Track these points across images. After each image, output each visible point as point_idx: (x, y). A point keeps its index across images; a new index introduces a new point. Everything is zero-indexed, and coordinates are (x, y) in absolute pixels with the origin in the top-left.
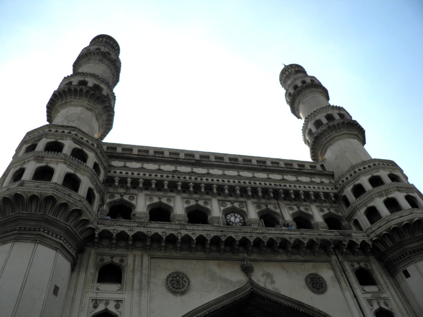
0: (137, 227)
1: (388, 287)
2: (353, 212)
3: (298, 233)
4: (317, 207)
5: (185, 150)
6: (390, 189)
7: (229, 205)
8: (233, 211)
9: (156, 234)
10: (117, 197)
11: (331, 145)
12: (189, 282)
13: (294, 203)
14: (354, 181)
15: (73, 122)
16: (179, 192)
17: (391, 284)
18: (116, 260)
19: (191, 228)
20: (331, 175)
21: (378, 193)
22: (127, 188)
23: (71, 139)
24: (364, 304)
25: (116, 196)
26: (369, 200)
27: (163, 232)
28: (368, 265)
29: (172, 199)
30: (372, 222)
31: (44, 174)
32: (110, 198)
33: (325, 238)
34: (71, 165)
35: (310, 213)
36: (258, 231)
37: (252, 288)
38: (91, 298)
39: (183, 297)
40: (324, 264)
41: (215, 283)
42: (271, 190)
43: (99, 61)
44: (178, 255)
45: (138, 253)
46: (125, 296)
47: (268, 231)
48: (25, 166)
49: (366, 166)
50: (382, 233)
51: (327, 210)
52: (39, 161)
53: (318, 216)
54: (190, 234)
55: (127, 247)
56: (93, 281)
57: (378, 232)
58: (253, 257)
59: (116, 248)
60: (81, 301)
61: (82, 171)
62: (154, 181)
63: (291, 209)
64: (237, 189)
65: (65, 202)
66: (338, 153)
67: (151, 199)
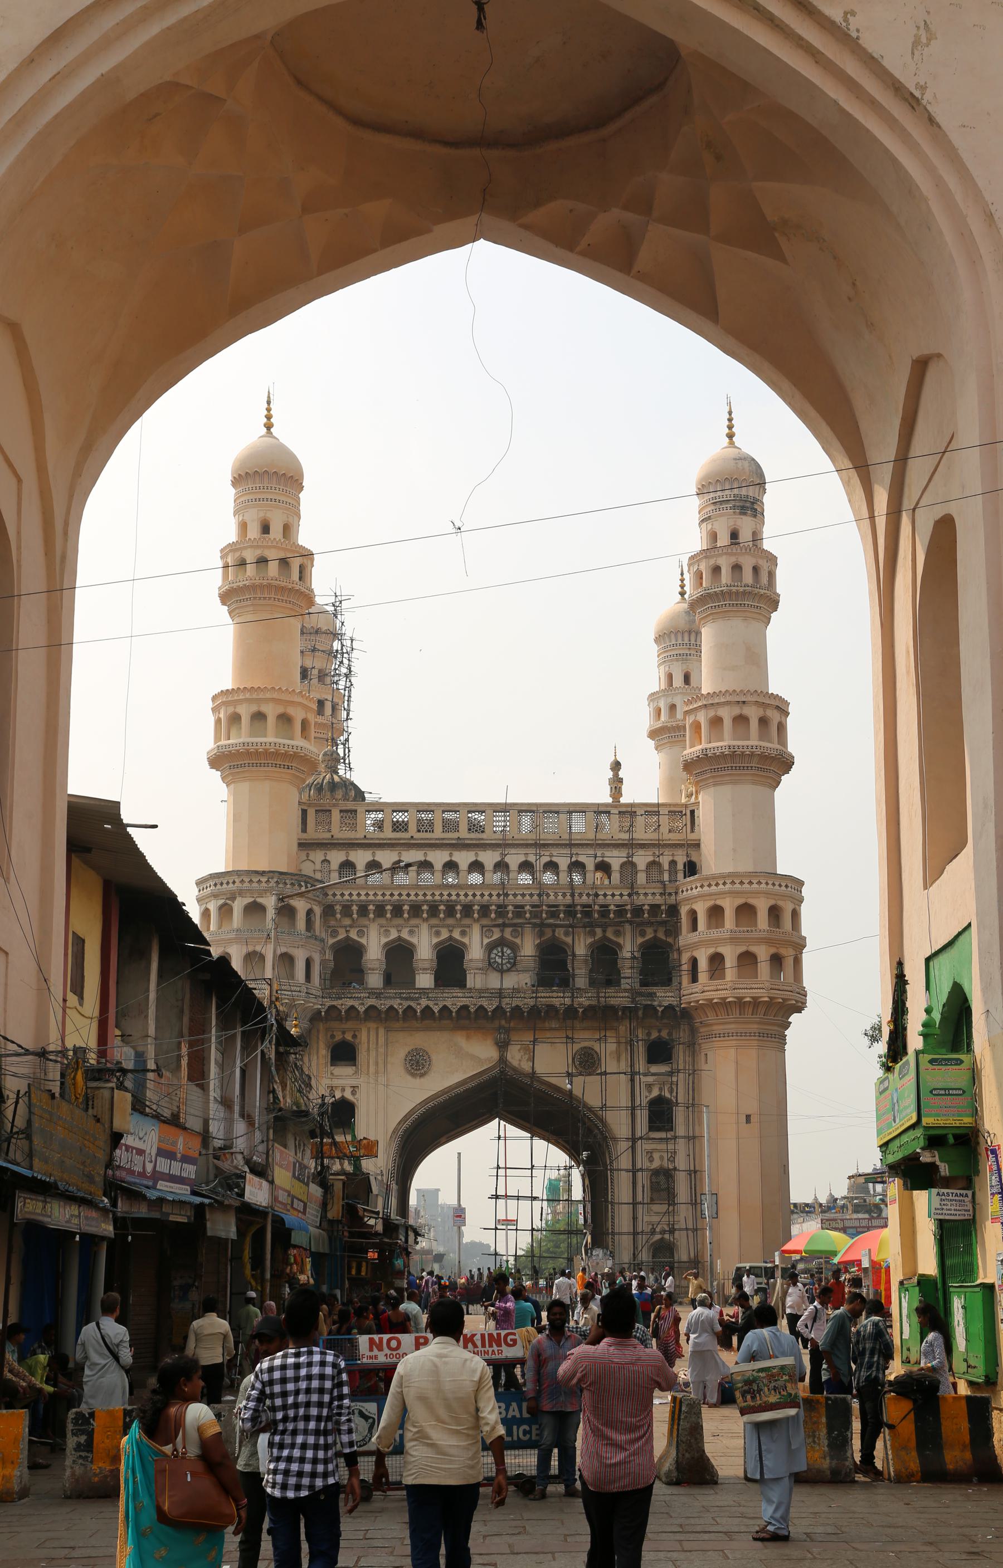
7: (496, 935)
9: (391, 1008)
12: (430, 1061)
18: (349, 1037)
20: (697, 845)
27: (400, 1004)
35: (621, 941)
39: (422, 1079)
41: (460, 1061)
42: (561, 908)
45: (372, 1025)
46: (361, 1081)
53: (629, 946)
54: (431, 1004)
56: (326, 1066)
58: (512, 1025)
63: (593, 934)
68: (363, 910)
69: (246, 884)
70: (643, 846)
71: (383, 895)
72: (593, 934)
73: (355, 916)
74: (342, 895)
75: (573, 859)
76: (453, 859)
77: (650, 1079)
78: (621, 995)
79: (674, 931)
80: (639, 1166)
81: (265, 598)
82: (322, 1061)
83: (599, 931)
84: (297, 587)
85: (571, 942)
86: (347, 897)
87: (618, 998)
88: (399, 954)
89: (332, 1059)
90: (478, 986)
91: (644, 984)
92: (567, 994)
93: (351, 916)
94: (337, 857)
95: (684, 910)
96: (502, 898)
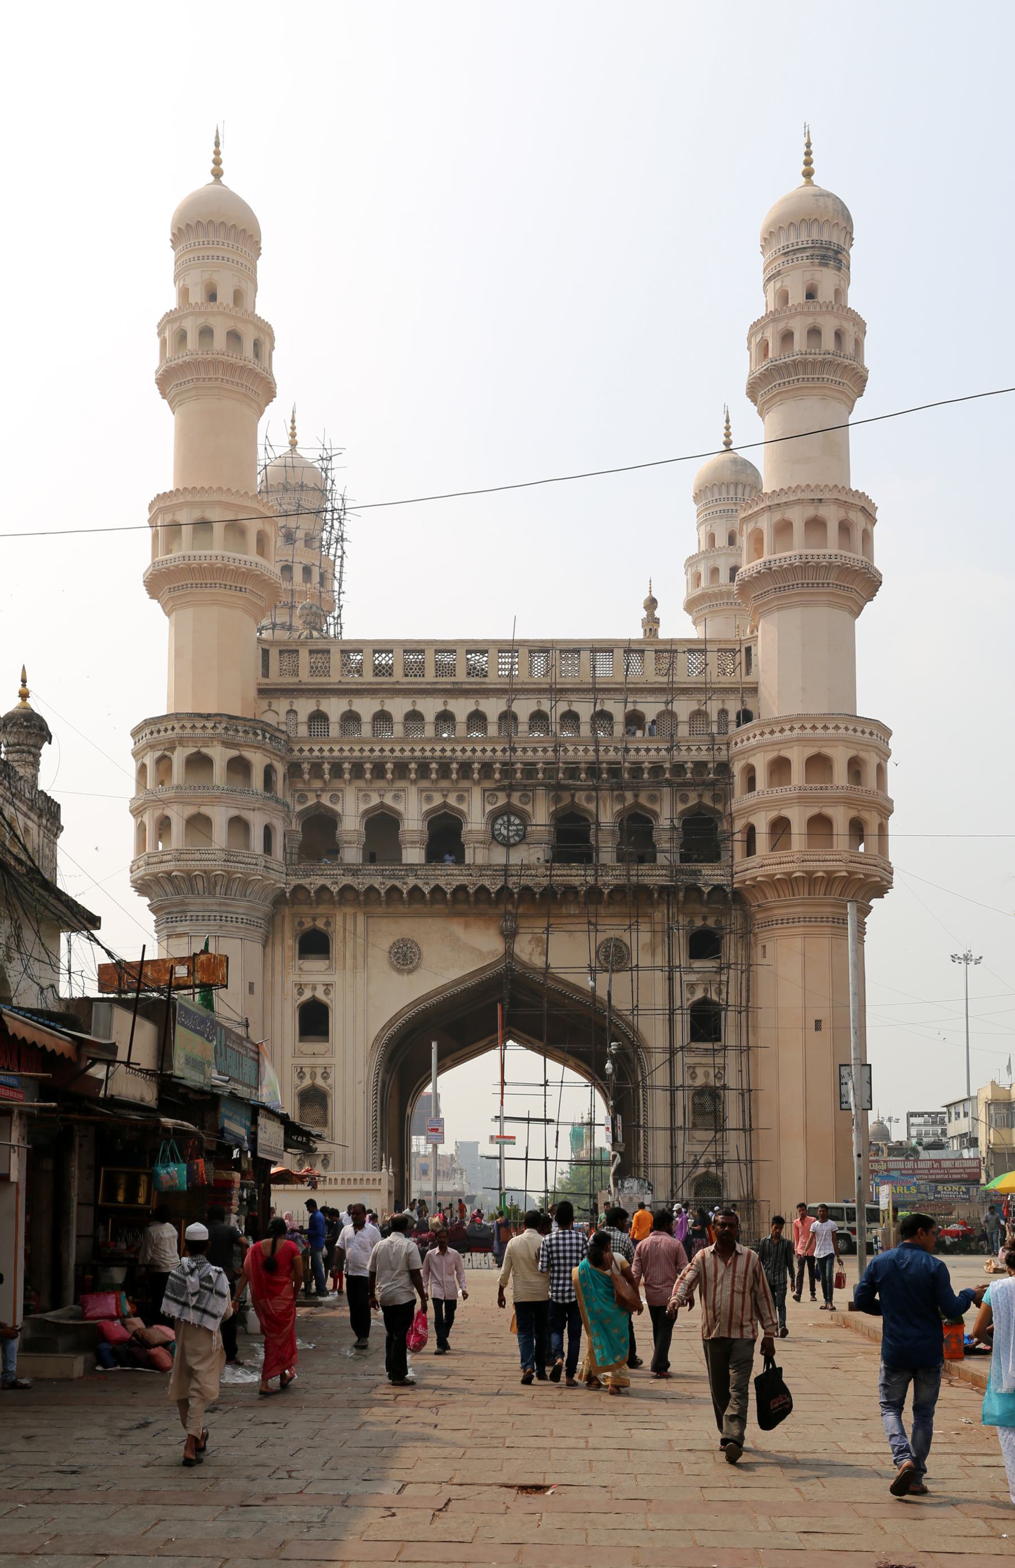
5: (436, 641)
7: (502, 800)
10: (312, 801)
12: (420, 954)
16: (414, 782)
18: (320, 924)
20: (754, 690)
29: (402, 794)
35: (656, 808)
36: (529, 872)
39: (411, 976)
41: (456, 955)
45: (349, 910)
46: (335, 978)
53: (666, 813)
54: (420, 883)
55: (331, 901)
58: (520, 910)
63: (621, 799)
68: (337, 770)
69: (188, 731)
70: (685, 691)
71: (362, 750)
72: (621, 799)
73: (327, 776)
74: (311, 750)
75: (598, 708)
76: (449, 708)
77: (693, 978)
78: (657, 872)
79: (724, 795)
80: (679, 1082)
81: (210, 379)
83: (629, 795)
84: (251, 366)
85: (594, 810)
86: (316, 753)
87: (653, 876)
88: (382, 826)
90: (480, 860)
91: (685, 858)
92: (589, 872)
93: (322, 777)
94: (305, 707)
95: (737, 768)
96: (508, 754)
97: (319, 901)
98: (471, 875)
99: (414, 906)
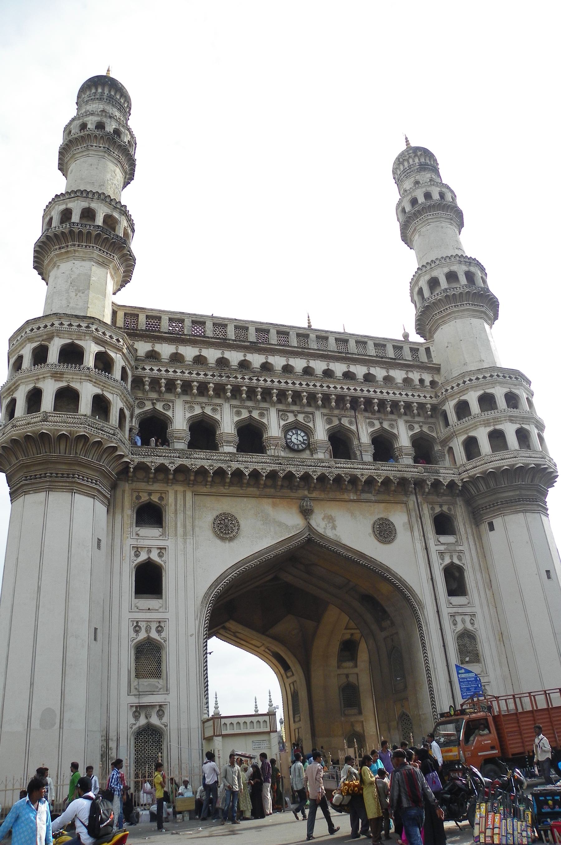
0: (179, 457)
1: (467, 538)
2: (449, 438)
3: (373, 467)
4: (406, 422)
5: (236, 320)
6: (500, 417)
7: (291, 418)
8: (295, 426)
9: (202, 467)
10: (148, 406)
11: (444, 323)
13: (377, 415)
14: (461, 394)
15: (83, 293)
16: (227, 399)
17: (473, 535)
19: (244, 459)
20: (437, 369)
21: (484, 421)
22: (160, 392)
23: (91, 338)
24: (434, 557)
25: (146, 405)
26: (472, 428)
28: (452, 508)
30: (469, 456)
31: (67, 398)
32: (139, 407)
33: (405, 476)
34: (98, 382)
35: (395, 431)
36: (324, 464)
37: (309, 534)
38: (132, 546)
39: (232, 544)
40: (399, 506)
42: (348, 398)
43: (105, 152)
44: (225, 491)
45: (180, 488)
46: (168, 543)
47: (336, 463)
48: (40, 385)
49: (480, 376)
50: (476, 474)
51: (418, 427)
52: (58, 379)
54: (241, 467)
55: (166, 481)
57: (472, 473)
58: (314, 495)
59: (154, 482)
60: (121, 548)
61: (111, 388)
62: (195, 383)
63: (372, 424)
64: (304, 396)
65: (100, 440)
66: (453, 331)
67: (191, 408)
82: (127, 521)
85: (356, 430)
89: (137, 523)
94: (143, 347)
97: (155, 480)
98: (280, 464)
99: (231, 488)
